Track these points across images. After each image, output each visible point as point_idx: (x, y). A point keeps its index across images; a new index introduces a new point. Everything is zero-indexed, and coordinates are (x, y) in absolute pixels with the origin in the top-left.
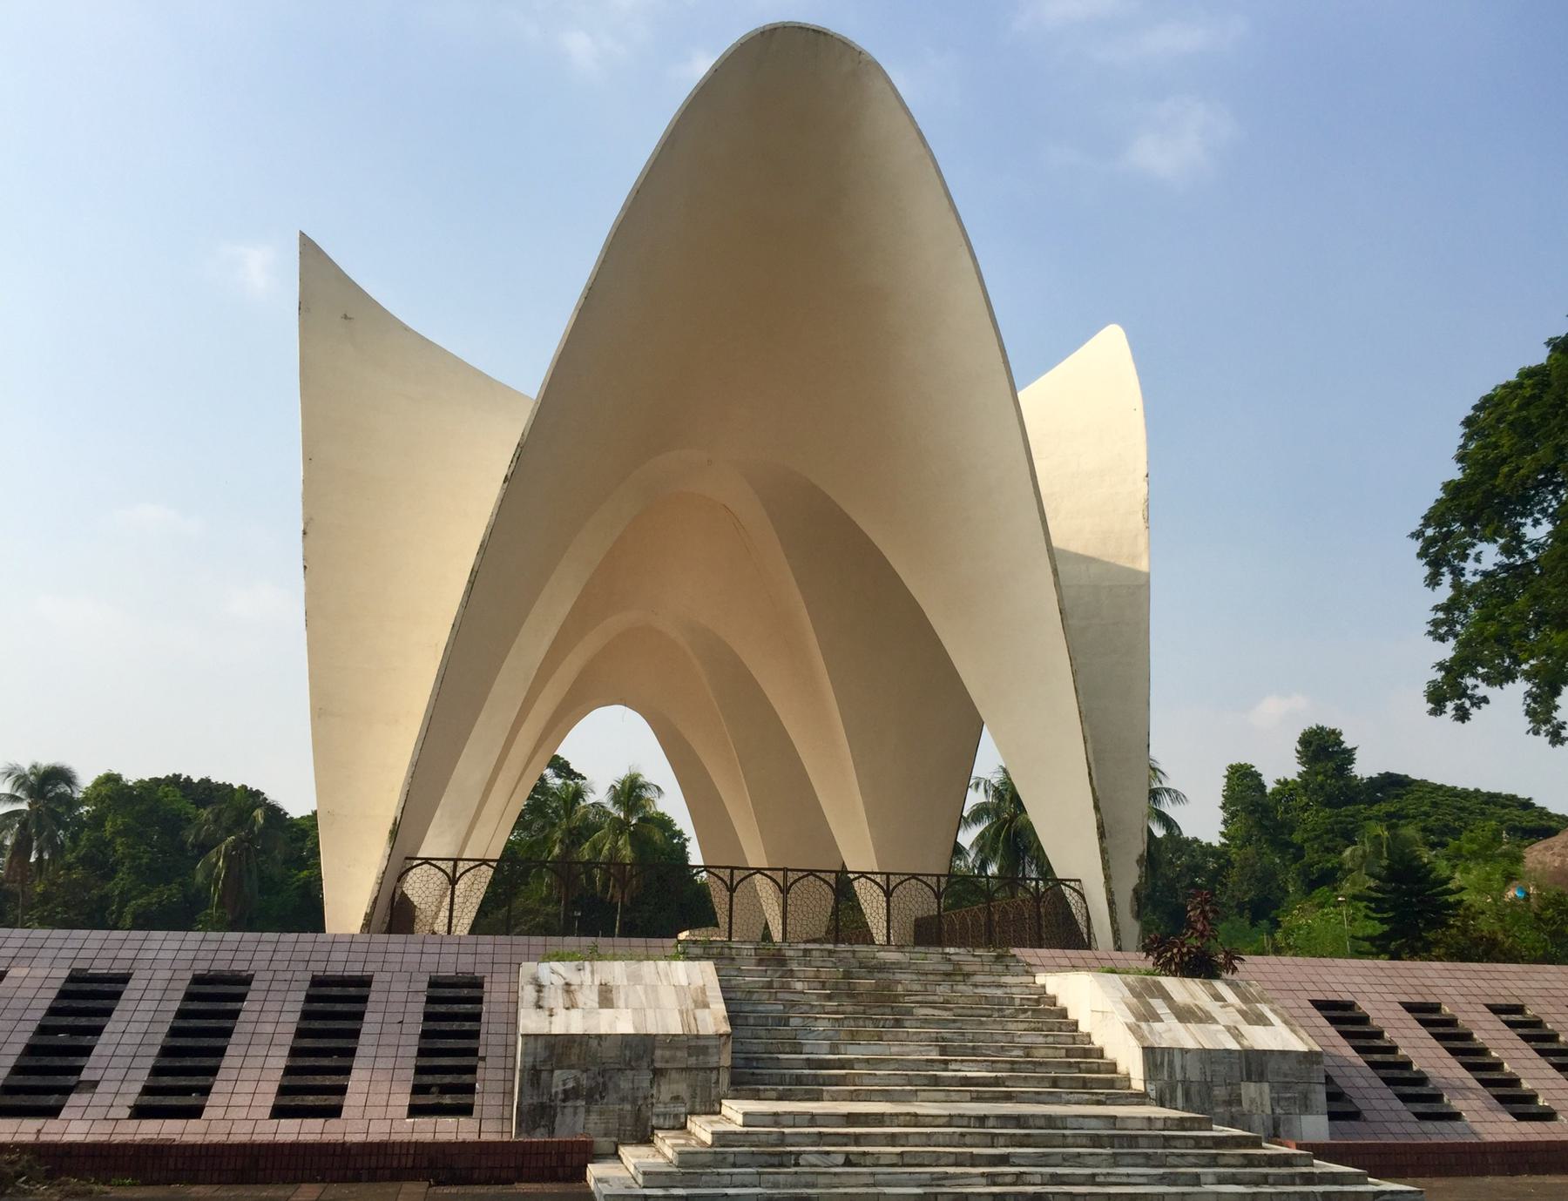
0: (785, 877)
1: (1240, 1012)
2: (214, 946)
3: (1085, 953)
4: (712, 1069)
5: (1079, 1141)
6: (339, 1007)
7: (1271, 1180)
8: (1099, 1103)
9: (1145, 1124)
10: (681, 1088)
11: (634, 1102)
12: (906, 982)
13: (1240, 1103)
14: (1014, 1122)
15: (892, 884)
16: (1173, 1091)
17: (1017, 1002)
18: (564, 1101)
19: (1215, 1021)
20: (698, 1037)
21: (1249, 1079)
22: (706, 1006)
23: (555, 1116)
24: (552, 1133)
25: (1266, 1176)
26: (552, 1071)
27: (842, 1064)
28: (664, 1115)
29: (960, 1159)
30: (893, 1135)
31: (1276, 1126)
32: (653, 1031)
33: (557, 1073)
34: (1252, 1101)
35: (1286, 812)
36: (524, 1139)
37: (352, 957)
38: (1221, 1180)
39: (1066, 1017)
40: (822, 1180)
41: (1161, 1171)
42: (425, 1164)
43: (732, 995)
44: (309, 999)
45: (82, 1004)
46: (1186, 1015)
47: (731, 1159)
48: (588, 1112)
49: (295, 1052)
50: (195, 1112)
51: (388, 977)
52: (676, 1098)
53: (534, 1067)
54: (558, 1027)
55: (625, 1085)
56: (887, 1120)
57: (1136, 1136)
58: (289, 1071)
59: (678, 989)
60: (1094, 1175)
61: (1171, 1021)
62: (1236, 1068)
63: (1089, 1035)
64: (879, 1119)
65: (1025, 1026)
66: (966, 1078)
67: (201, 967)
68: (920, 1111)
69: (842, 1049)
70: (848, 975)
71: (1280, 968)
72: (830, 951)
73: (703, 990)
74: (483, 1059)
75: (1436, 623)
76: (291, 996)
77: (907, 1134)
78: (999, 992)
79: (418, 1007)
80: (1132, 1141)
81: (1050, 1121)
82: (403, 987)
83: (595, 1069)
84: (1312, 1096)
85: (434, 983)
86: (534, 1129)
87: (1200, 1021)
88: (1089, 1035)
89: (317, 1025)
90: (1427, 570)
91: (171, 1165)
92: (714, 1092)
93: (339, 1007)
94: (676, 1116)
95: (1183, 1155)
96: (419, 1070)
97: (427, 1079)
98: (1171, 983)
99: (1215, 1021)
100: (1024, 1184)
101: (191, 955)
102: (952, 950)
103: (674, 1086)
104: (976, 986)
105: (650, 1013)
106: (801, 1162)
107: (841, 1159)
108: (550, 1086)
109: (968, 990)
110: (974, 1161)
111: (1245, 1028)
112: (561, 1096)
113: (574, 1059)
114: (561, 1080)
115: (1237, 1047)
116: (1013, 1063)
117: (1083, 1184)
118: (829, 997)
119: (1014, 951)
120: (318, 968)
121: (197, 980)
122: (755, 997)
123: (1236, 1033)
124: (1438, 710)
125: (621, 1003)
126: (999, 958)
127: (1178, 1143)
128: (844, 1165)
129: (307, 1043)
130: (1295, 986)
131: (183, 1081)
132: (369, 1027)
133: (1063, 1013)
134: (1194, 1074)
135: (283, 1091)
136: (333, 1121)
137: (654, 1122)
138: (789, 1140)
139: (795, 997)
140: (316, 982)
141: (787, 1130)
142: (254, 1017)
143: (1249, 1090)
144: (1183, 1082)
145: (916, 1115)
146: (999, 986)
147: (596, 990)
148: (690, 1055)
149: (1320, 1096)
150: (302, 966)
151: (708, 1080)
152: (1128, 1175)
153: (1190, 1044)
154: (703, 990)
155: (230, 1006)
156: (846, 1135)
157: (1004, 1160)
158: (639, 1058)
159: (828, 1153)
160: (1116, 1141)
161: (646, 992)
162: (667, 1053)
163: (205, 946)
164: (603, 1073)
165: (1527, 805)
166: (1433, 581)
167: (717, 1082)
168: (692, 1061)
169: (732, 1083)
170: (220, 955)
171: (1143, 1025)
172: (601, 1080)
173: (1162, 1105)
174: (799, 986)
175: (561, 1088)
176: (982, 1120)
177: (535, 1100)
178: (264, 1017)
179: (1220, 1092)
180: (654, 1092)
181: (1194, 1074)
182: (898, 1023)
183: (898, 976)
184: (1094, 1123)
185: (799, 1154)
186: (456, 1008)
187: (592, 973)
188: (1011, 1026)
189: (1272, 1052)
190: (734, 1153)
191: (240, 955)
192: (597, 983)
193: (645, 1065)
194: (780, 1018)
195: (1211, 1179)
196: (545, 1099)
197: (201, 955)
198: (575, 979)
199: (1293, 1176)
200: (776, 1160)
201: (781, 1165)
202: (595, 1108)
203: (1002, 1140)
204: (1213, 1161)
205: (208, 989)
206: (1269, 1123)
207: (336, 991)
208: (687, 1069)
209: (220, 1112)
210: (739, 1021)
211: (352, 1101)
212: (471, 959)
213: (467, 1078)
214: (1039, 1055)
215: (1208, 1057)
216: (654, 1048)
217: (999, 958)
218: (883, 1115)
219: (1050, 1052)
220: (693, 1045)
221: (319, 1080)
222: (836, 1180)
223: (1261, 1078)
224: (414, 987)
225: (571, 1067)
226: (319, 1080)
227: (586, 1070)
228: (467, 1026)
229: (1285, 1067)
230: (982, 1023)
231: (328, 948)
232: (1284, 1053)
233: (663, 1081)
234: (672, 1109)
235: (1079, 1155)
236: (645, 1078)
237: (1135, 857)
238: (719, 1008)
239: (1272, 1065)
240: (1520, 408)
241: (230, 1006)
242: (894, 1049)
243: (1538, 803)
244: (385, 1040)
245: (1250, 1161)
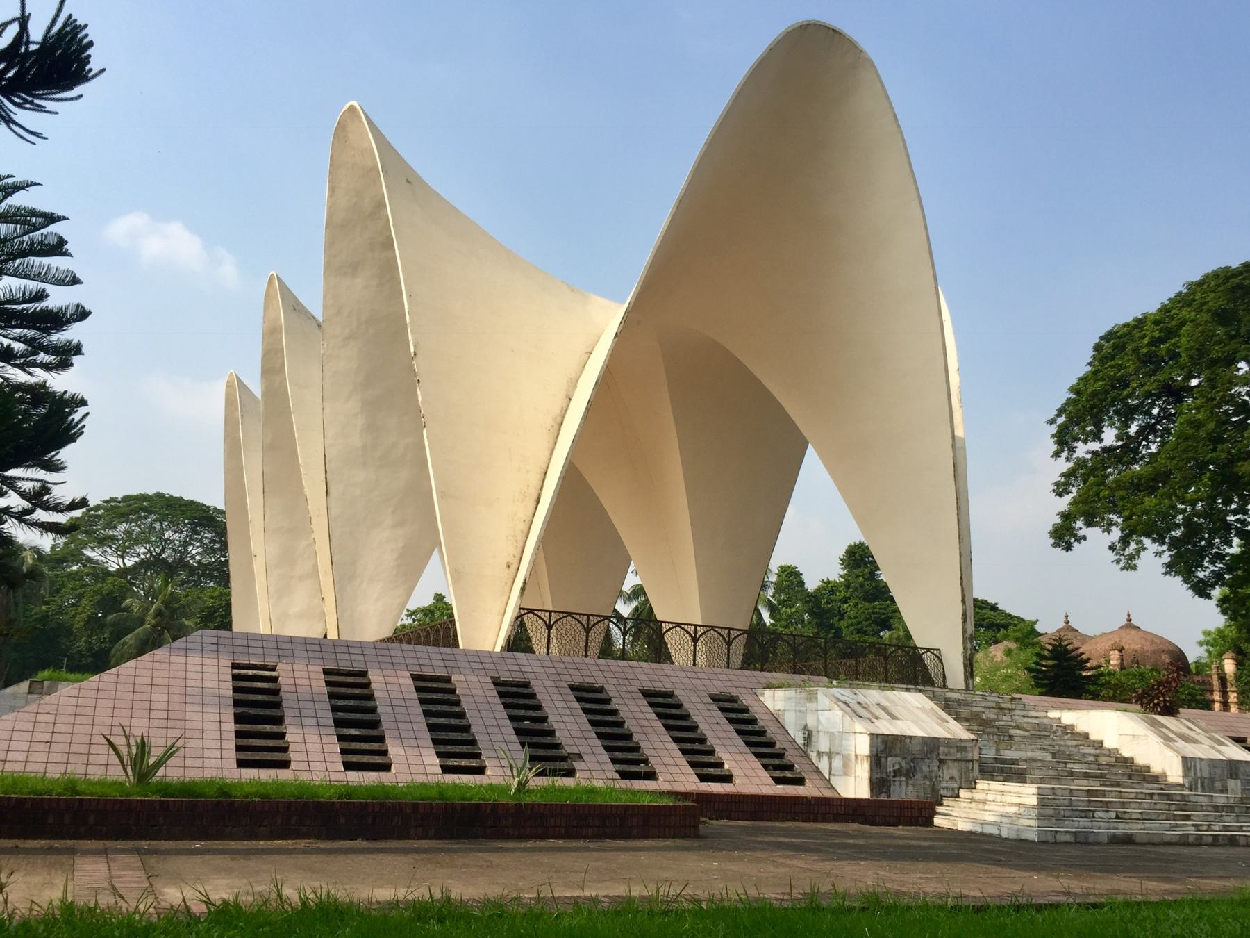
10: (955, 773)
11: (931, 780)
20: (961, 740)
35: (828, 603)
45: (522, 701)
55: (925, 769)
75: (1057, 484)
90: (1055, 447)
107: (1113, 815)
108: (886, 767)
114: (892, 763)
124: (1068, 548)
134: (1206, 775)
137: (942, 792)
153: (1202, 756)
158: (931, 752)
162: (946, 750)
164: (913, 760)
165: (994, 608)
166: (1057, 455)
168: (959, 756)
169: (980, 771)
179: (1218, 785)
181: (1206, 775)
203: (1173, 807)
223: (1237, 777)
225: (896, 756)
233: (945, 768)
239: (1242, 769)
240: (1149, 344)
243: (1001, 607)
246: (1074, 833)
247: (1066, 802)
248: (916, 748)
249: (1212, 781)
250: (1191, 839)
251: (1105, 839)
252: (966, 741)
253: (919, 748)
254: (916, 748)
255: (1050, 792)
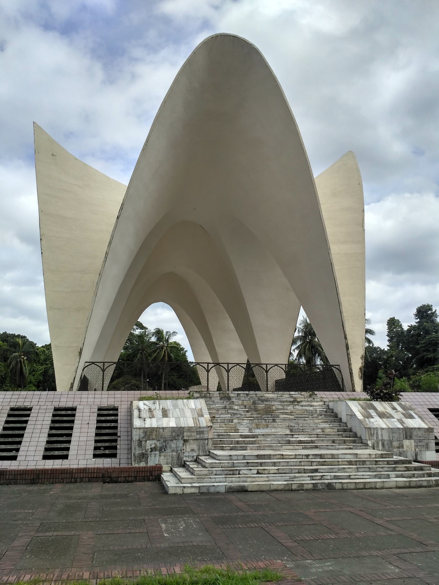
0: (228, 366)
1: (403, 414)
2: (17, 397)
3: (342, 393)
4: (205, 439)
5: (344, 463)
6: (65, 418)
7: (416, 476)
8: (350, 449)
9: (368, 456)
10: (195, 447)
12: (276, 405)
13: (403, 447)
14: (319, 457)
15: (268, 368)
16: (378, 443)
17: (318, 412)
18: (151, 452)
19: (393, 418)
20: (200, 428)
21: (406, 438)
22: (202, 416)
23: (148, 457)
24: (147, 463)
25: (414, 474)
26: (146, 441)
27: (254, 437)
28: (188, 456)
29: (300, 471)
30: (274, 462)
31: (416, 456)
32: (183, 426)
33: (148, 442)
34: (407, 446)
36: (137, 465)
37: (68, 400)
38: (397, 476)
39: (337, 417)
40: (249, 479)
41: (375, 473)
42: (101, 476)
43: (211, 411)
44: (54, 416)
46: (382, 415)
47: (215, 472)
48: (160, 455)
49: (50, 435)
50: (14, 458)
51: (81, 407)
52: (193, 450)
53: (139, 440)
54: (147, 426)
56: (272, 457)
57: (365, 461)
58: (48, 442)
59: (192, 410)
60: (350, 476)
61: (377, 418)
62: (402, 435)
63: (346, 423)
64: (269, 457)
65: (321, 421)
66: (300, 441)
67: (13, 405)
68: (284, 453)
69: (253, 431)
70: (254, 403)
71: (417, 397)
72: (247, 394)
73: (201, 410)
74: (120, 437)
76: (47, 415)
77: (280, 462)
78: (311, 408)
79: (94, 418)
80: (364, 462)
81: (333, 456)
82: (88, 410)
83: (162, 440)
84: (430, 444)
85: (99, 409)
86: (140, 462)
87: (388, 418)
88: (346, 423)
89: (57, 425)
91: (7, 478)
92: (206, 448)
93: (65, 418)
94: (193, 457)
95: (383, 467)
96: (96, 441)
97: (99, 445)
98: (376, 404)
99: (393, 418)
100: (324, 479)
101: (9, 400)
102: (293, 393)
103: (192, 446)
104: (302, 406)
105: (182, 419)
106: (241, 473)
107: (255, 472)
109: (300, 408)
110: (305, 471)
111: (405, 420)
112: (150, 450)
113: (154, 437)
114: (149, 444)
115: (402, 427)
116: (318, 434)
117: (346, 479)
118: (248, 412)
119: (316, 392)
120: (56, 404)
121: (12, 409)
122: (220, 412)
123: (401, 422)
125: (171, 416)
126: (310, 396)
127: (380, 463)
128: (257, 474)
129: (54, 432)
130: (422, 403)
131: (9, 447)
132: (76, 425)
133: (336, 416)
134: (386, 437)
135: (46, 449)
136: (65, 460)
137: (185, 459)
138: (235, 465)
139: (235, 412)
140: (56, 409)
141: (235, 462)
142: (34, 423)
143: (406, 443)
144: (382, 440)
145: (283, 455)
146: (311, 406)
147: (161, 411)
148: (197, 434)
149: (432, 444)
150: (50, 403)
151: (204, 443)
152: (363, 475)
153: (384, 426)
154: (201, 410)
155: (24, 419)
156: (257, 463)
157: (316, 471)
158: (178, 436)
159: (251, 470)
160: (358, 463)
161: (180, 411)
162: (189, 434)
163: (14, 397)
164: (165, 441)
167: (208, 444)
168: (198, 437)
170: (19, 400)
171: (367, 420)
172: (164, 444)
173: (374, 449)
174: (236, 407)
175: (149, 447)
176: (307, 456)
177: (140, 452)
178: (37, 423)
179: (395, 444)
180: (184, 448)
181: (386, 437)
182: (274, 421)
183: (273, 403)
184: (349, 456)
185: (240, 470)
186: (108, 418)
187: (159, 404)
188: (316, 421)
189: (415, 428)
190: (216, 470)
191: (26, 400)
192: (161, 408)
193: (180, 438)
194: (230, 420)
195: (394, 476)
196: (144, 451)
197: (12, 400)
198: (153, 407)
199: (424, 474)
200: (231, 473)
201: (233, 474)
202: (162, 454)
203: (315, 464)
204: (394, 470)
205: (16, 413)
206: (414, 455)
207: (63, 413)
208: (197, 439)
209: (23, 458)
210: (214, 421)
211: (71, 453)
212: (113, 400)
213: (114, 444)
214: (328, 431)
215: (392, 430)
216: (183, 432)
217: (310, 396)
218: (270, 455)
219: (331, 430)
220: (199, 431)
221: (59, 446)
222: (254, 479)
223: (411, 438)
224: (92, 411)
225: (153, 439)
226: (59, 446)
227: (159, 440)
228: (113, 425)
229: (420, 433)
230: (305, 420)
231: (59, 396)
232: (419, 429)
233: (187, 444)
234: (191, 454)
235: (344, 468)
236: (181, 443)
237: (360, 356)
238: (207, 416)
239: (415, 433)
241: (24, 419)
242: (273, 430)
244: (83, 430)
245: (408, 469)
246: (199, 487)
247: (230, 465)
248: (167, 434)
249: (391, 442)
250: (294, 487)
251: (223, 490)
252: (203, 428)
253: (169, 434)
254: (167, 434)
255: (228, 458)
